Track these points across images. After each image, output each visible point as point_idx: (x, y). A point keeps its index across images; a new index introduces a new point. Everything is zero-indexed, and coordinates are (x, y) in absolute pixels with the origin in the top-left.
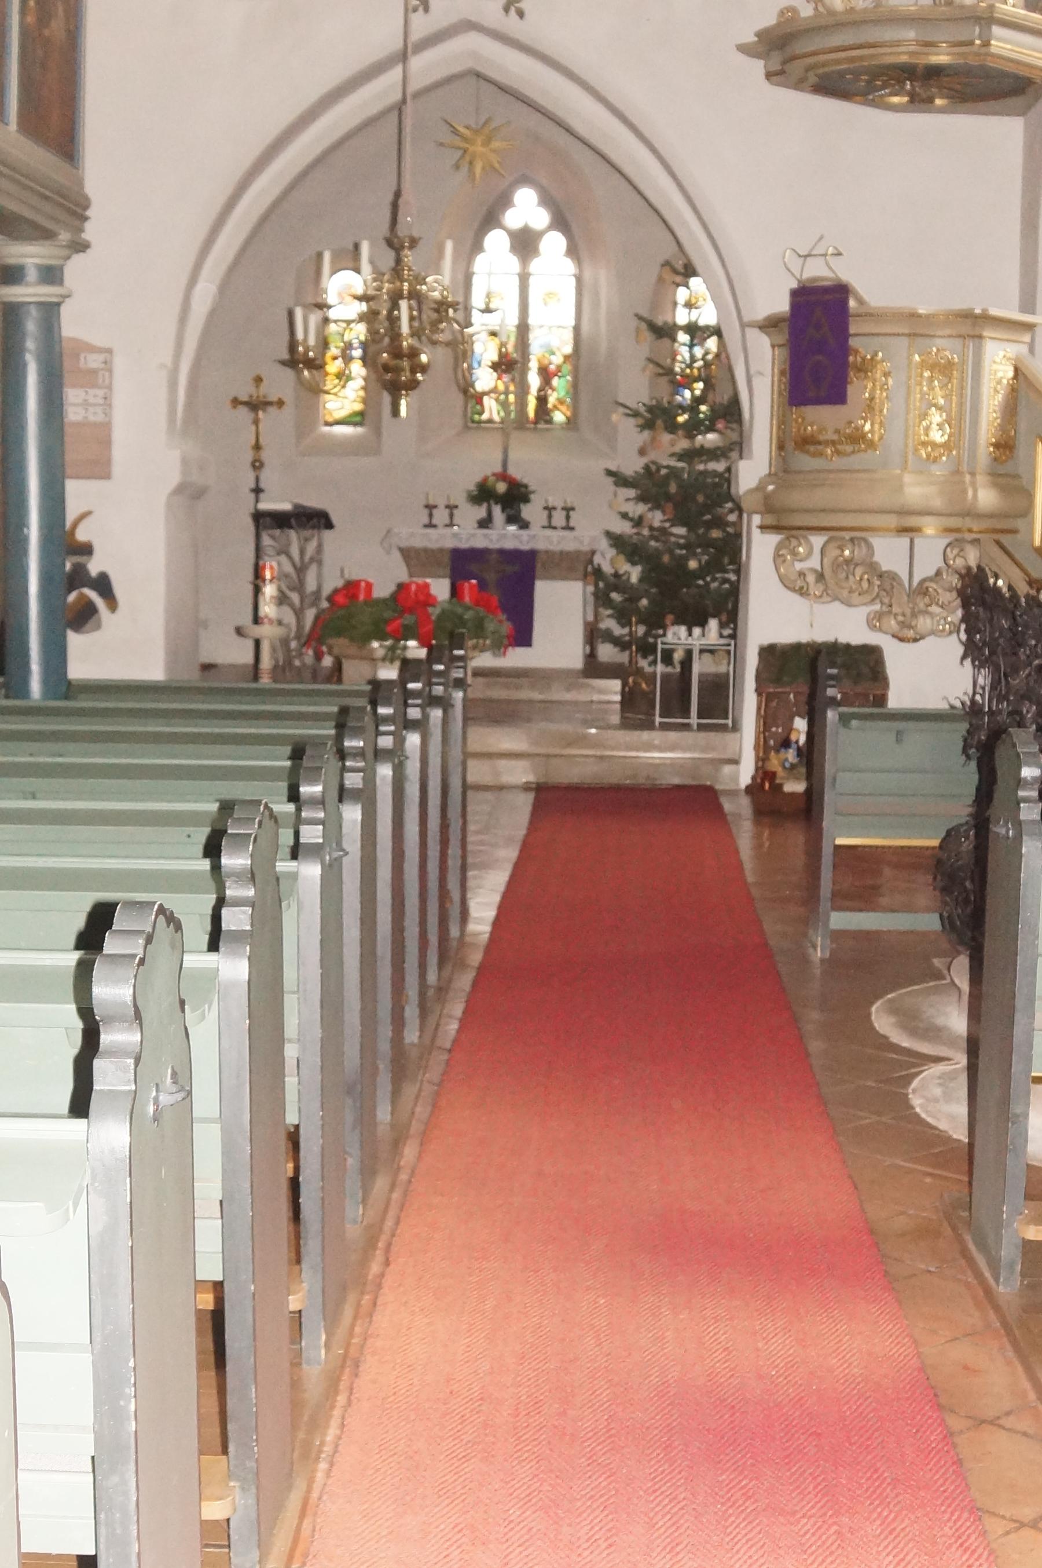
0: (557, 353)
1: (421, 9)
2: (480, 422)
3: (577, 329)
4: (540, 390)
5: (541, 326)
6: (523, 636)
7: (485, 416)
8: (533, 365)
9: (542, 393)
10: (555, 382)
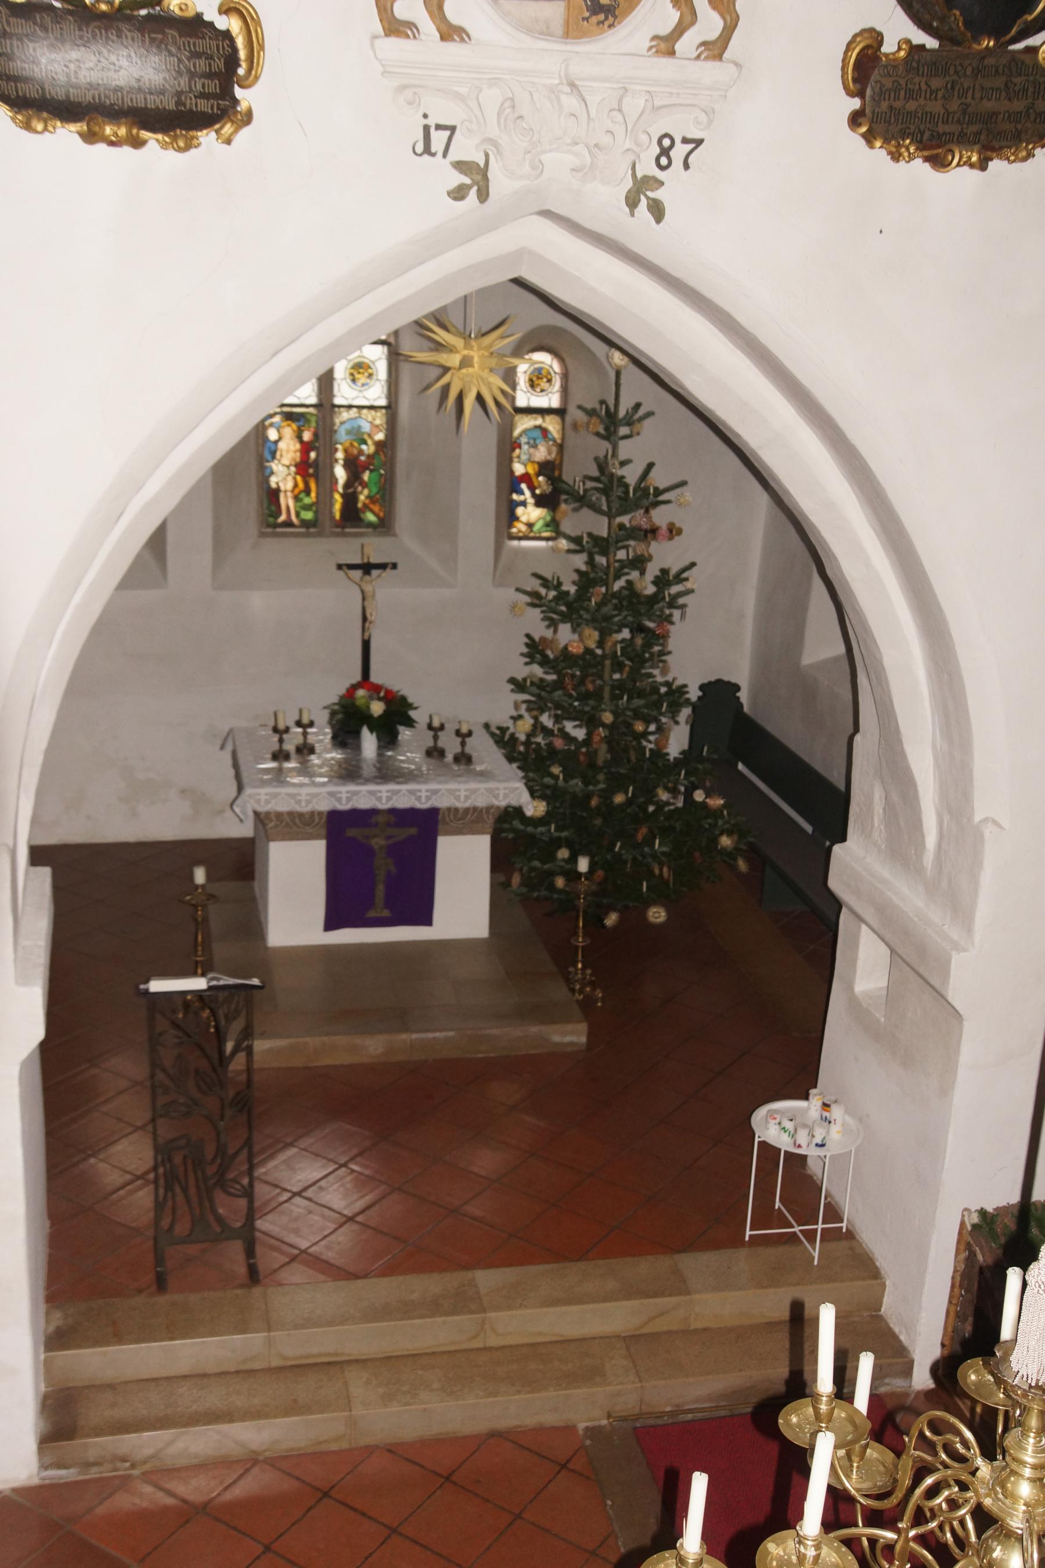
0: (370, 442)
1: (473, 192)
2: (276, 526)
3: (391, 409)
4: (347, 486)
5: (350, 407)
6: (425, 918)
7: (283, 518)
8: (340, 455)
9: (351, 490)
10: (366, 476)
